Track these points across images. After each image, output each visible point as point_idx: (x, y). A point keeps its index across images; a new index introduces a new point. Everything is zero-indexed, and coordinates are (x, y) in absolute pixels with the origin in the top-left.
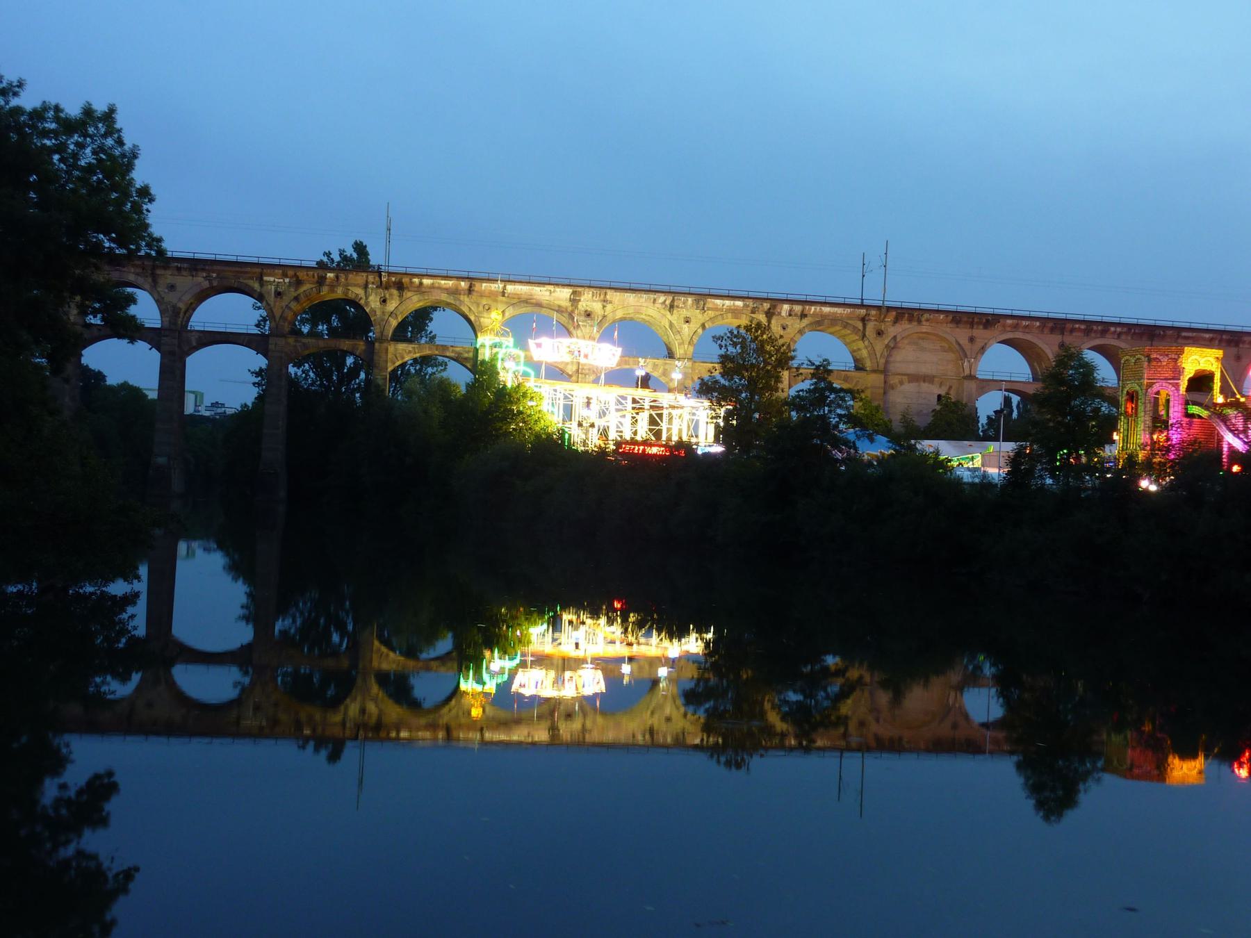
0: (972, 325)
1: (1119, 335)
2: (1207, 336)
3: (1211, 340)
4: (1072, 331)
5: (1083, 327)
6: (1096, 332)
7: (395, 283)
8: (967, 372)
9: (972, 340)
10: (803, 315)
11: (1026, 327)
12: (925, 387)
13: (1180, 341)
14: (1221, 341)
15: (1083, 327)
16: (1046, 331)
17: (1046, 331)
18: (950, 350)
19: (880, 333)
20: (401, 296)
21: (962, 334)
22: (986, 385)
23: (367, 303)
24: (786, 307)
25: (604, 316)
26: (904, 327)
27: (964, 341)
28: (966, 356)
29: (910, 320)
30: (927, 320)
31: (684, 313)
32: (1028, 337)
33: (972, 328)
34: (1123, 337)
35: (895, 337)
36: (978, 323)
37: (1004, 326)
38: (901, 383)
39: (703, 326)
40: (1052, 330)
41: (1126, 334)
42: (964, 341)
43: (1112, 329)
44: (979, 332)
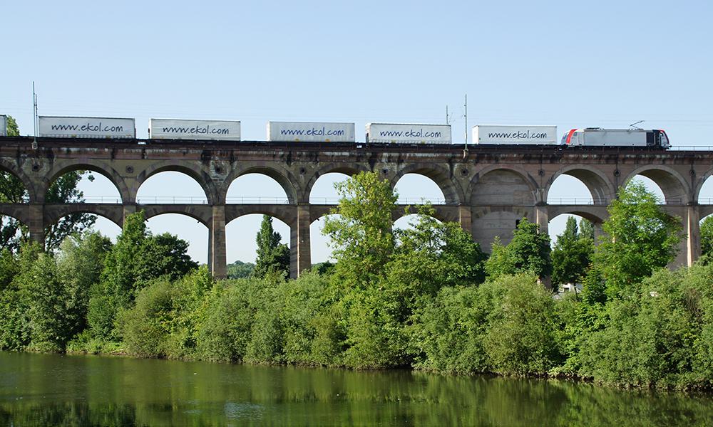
0: (540, 160)
1: (664, 160)
5: (633, 156)
6: (644, 159)
7: (44, 152)
9: (541, 173)
10: (400, 161)
11: (586, 159)
12: (504, 213)
15: (633, 156)
18: (524, 181)
19: (465, 172)
20: (51, 163)
21: (532, 169)
22: (555, 210)
23: (21, 171)
24: (385, 154)
27: (535, 175)
28: (537, 187)
29: (489, 159)
30: (503, 159)
32: (588, 168)
33: (541, 163)
34: (668, 162)
37: (567, 159)
38: (485, 212)
40: (607, 160)
41: (670, 159)
42: (535, 175)
43: (658, 156)
44: (546, 167)
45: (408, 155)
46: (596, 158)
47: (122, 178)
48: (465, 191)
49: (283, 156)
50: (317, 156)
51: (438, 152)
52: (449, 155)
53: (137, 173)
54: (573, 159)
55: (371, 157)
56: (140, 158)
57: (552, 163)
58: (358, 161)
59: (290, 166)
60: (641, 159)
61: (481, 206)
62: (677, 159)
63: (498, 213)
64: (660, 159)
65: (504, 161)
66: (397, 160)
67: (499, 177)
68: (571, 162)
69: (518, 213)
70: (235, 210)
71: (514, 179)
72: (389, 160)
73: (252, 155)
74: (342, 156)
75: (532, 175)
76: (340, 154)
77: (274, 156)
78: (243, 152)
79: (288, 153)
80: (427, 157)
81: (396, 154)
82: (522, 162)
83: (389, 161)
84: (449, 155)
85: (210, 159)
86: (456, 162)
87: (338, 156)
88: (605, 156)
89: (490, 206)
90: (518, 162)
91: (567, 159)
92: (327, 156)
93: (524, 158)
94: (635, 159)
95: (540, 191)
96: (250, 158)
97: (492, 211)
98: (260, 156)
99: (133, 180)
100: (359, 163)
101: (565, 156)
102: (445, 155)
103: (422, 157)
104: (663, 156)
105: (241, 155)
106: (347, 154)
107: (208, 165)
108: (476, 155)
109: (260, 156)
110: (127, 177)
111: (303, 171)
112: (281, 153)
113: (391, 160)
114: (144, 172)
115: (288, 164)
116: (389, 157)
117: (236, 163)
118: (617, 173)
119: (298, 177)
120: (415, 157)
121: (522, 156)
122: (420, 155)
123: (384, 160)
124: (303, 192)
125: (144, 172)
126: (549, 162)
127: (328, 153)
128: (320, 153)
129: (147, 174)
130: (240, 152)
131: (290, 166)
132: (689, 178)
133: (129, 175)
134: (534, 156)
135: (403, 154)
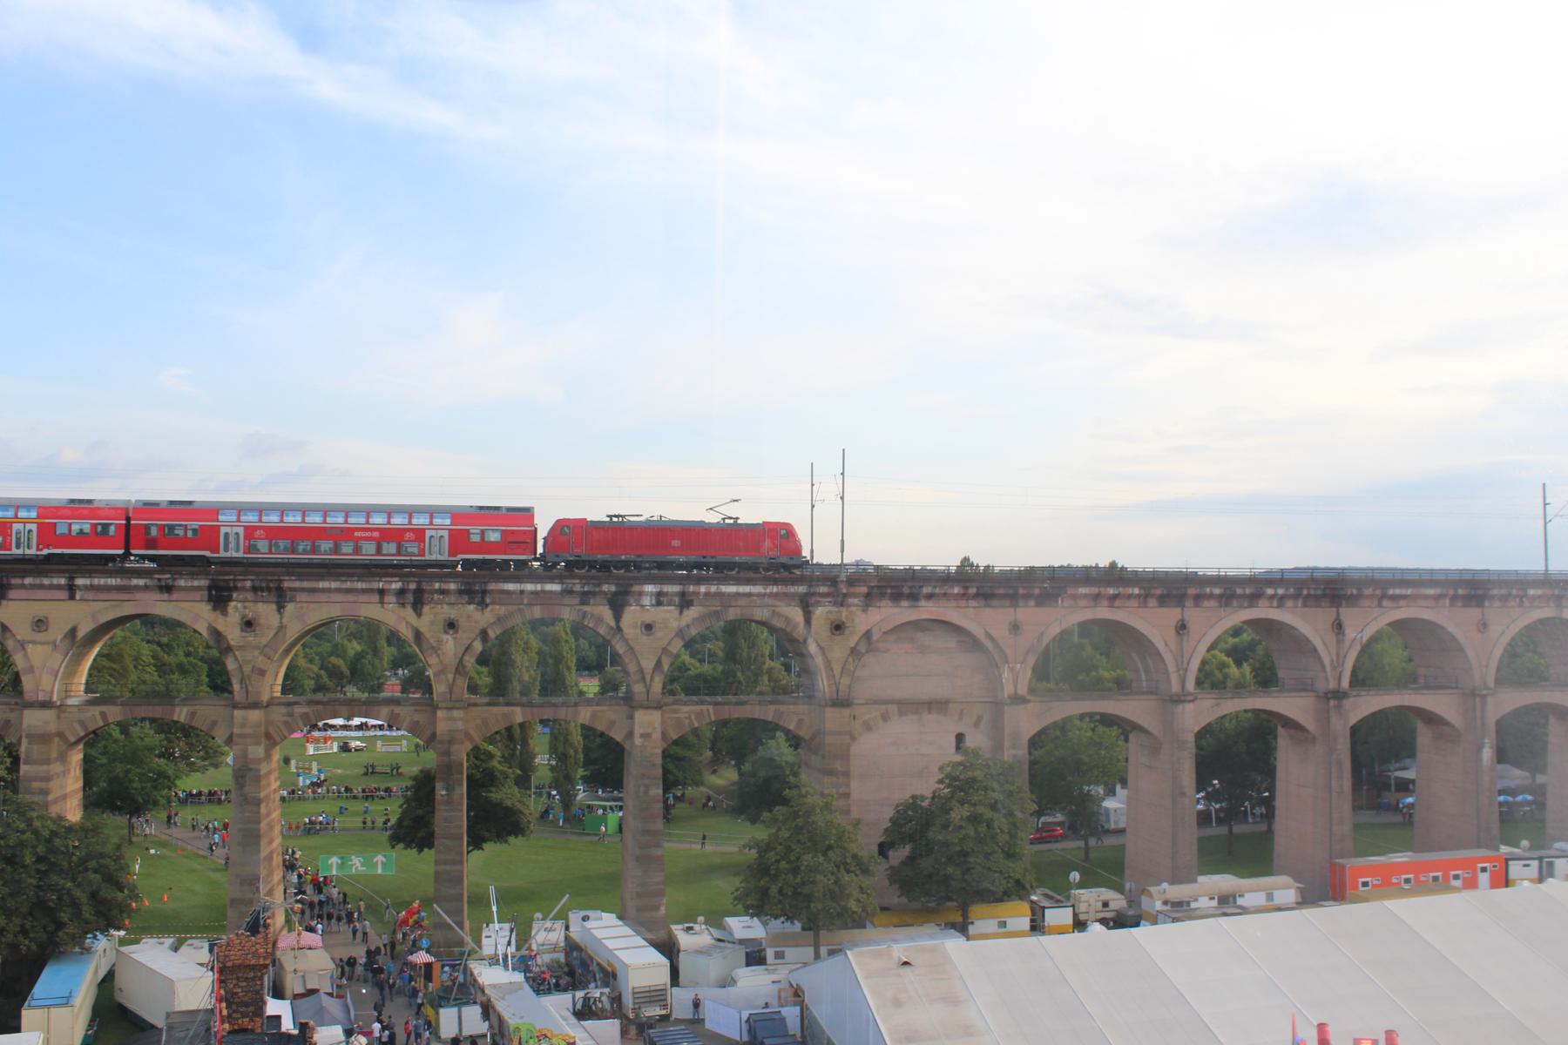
0: (1013, 599)
2: (1431, 592)
3: (1438, 598)
4: (1198, 598)
5: (1217, 591)
8: (1008, 690)
9: (1015, 628)
10: (685, 602)
11: (1115, 597)
12: (931, 719)
13: (1385, 603)
14: (1454, 598)
16: (1152, 602)
17: (1152, 602)
19: (838, 627)
24: (649, 588)
25: (282, 628)
26: (887, 614)
29: (897, 597)
30: (930, 597)
31: (448, 611)
33: (1015, 606)
35: (868, 635)
36: (1027, 596)
38: (885, 717)
39: (484, 635)
40: (1163, 600)
41: (1295, 597)
43: (1270, 591)
45: (703, 589)
46: (1139, 596)
47: (22, 645)
48: (837, 672)
49: (401, 593)
50: (484, 592)
51: (775, 582)
52: (802, 589)
53: (57, 632)
54: (1085, 596)
55: (615, 594)
56: (64, 594)
57: (1039, 604)
58: (584, 603)
59: (419, 615)
60: (1233, 596)
61: (875, 702)
62: (1308, 596)
63: (915, 717)
64: (1272, 597)
65: (931, 604)
66: (677, 600)
67: (920, 635)
68: (1082, 603)
69: (961, 719)
70: (291, 715)
71: (951, 642)
72: (659, 599)
73: (329, 590)
74: (543, 591)
75: (994, 634)
76: (539, 587)
77: (382, 592)
78: (306, 584)
79: (413, 586)
80: (749, 595)
81: (676, 588)
82: (973, 603)
83: (659, 603)
84: (802, 589)
85: (230, 599)
86: (818, 604)
87: (535, 593)
88: (1159, 592)
89: (899, 703)
90: (963, 603)
91: (1074, 597)
92: (508, 593)
93: (976, 596)
94: (1221, 596)
95: (1012, 670)
96: (323, 597)
97: (901, 714)
98: (349, 591)
99: (48, 648)
100: (586, 608)
101: (1070, 591)
102: (792, 589)
103: (738, 594)
104: (1280, 591)
105: (302, 590)
106: (556, 587)
107: (225, 613)
108: (864, 590)
109: (349, 591)
110: (34, 642)
111: (451, 625)
112: (396, 586)
113: (665, 600)
114: (73, 631)
115: (415, 610)
116: (659, 594)
117: (290, 607)
118: (1182, 627)
119: (440, 642)
120: (720, 594)
121: (973, 590)
122: (732, 589)
123: (646, 601)
124: (450, 677)
125: (73, 631)
126: (1032, 603)
127: (511, 587)
128: (492, 586)
129: (81, 634)
130: (297, 584)
131: (419, 615)
132: (1331, 638)
133: (40, 637)
134: (1001, 591)
135: (691, 588)
